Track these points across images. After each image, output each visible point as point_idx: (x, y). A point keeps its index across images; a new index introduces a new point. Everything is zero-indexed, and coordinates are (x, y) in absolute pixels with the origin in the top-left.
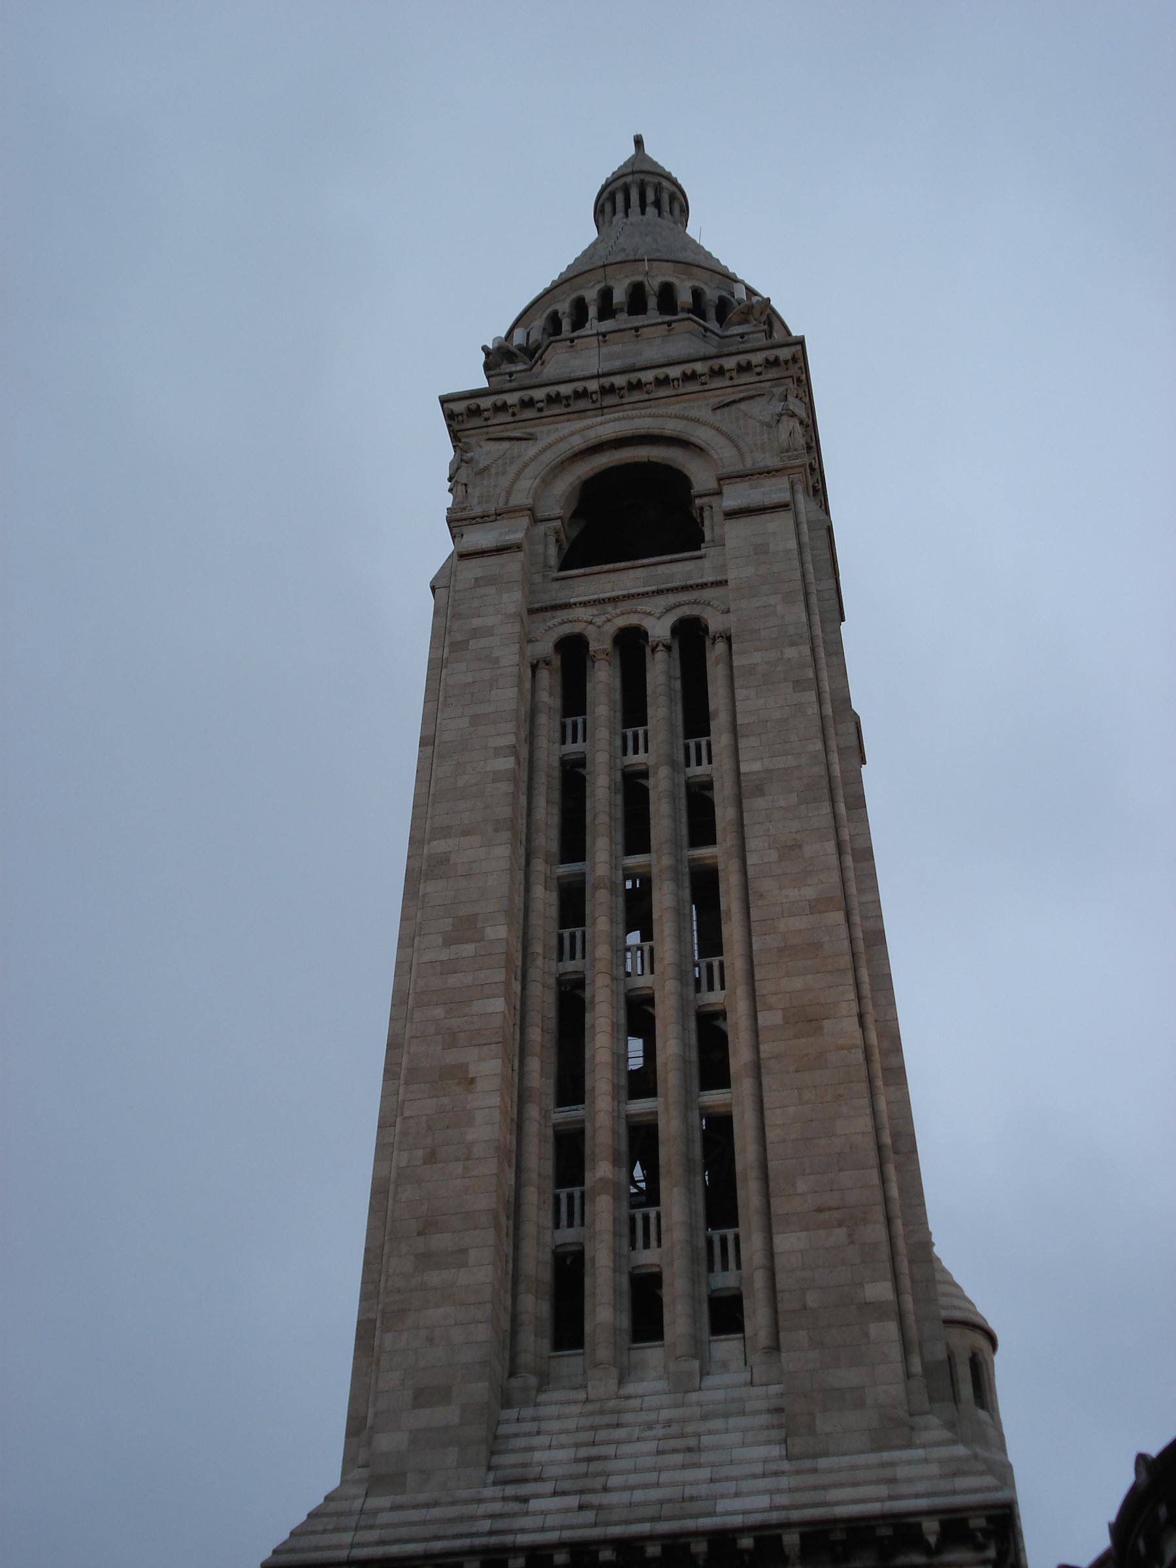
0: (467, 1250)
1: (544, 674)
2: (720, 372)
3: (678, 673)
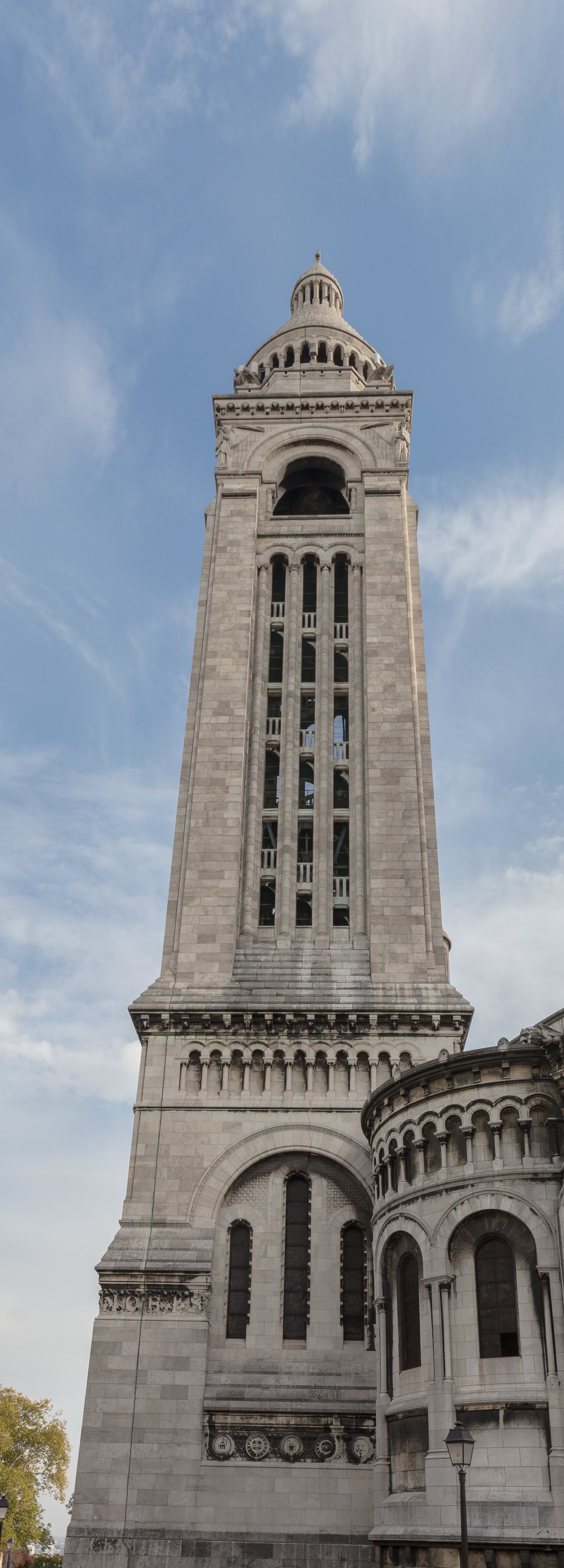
0: (224, 871)
1: (264, 573)
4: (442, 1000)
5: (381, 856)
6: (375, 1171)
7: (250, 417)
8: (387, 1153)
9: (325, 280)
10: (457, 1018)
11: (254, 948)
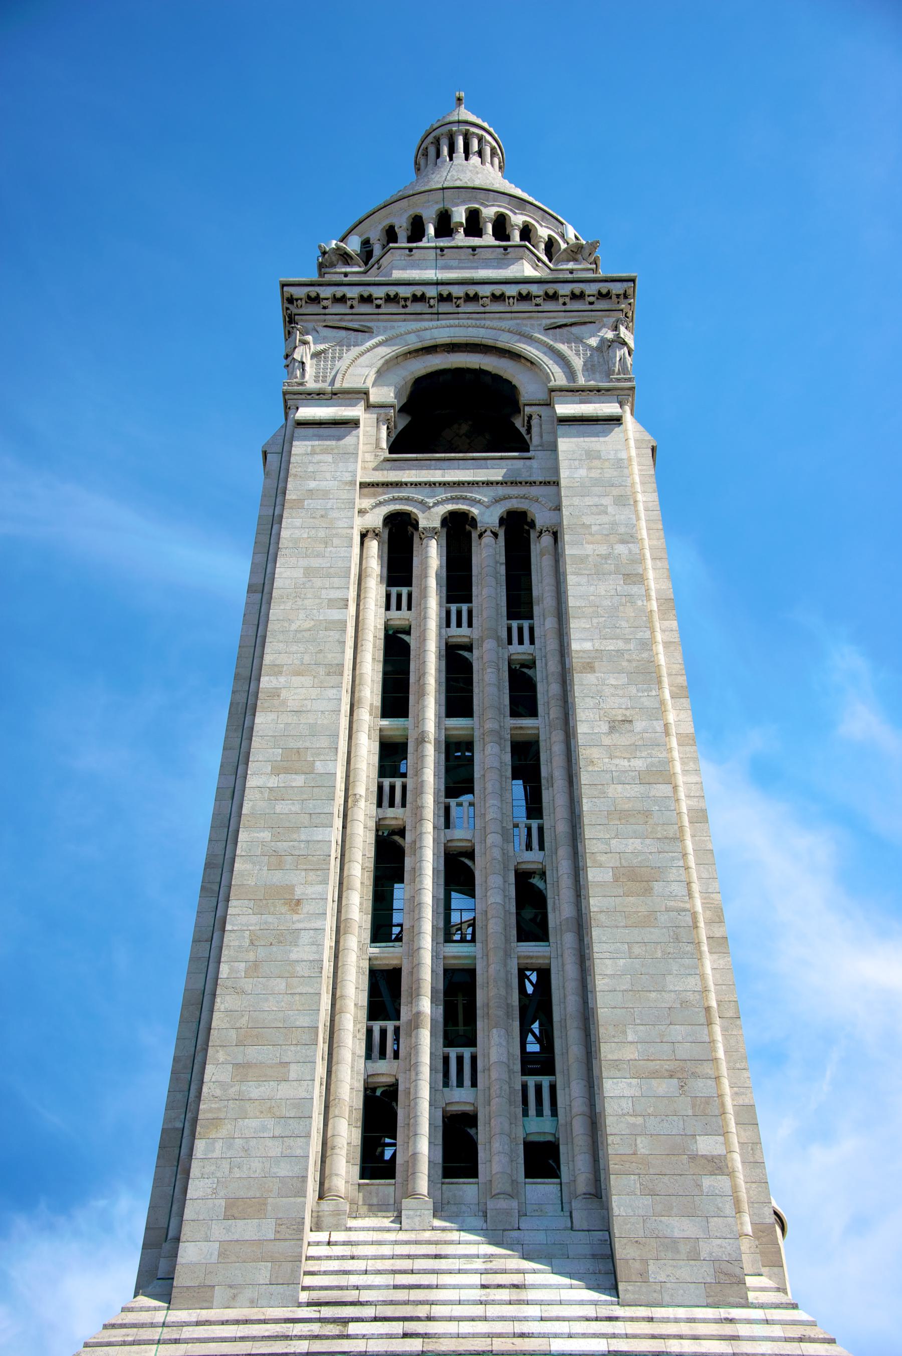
5: (624, 1033)
7: (349, 311)
11: (349, 1229)
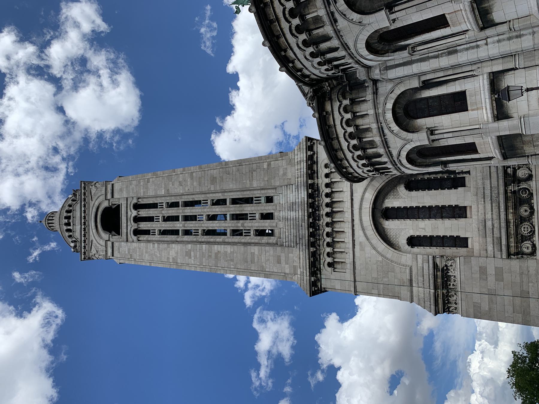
2: (85, 200)
3: (144, 210)
4: (302, 151)
5: (244, 183)
6: (378, 174)
7: (87, 245)
8: (369, 168)
9: (47, 219)
10: (309, 144)
